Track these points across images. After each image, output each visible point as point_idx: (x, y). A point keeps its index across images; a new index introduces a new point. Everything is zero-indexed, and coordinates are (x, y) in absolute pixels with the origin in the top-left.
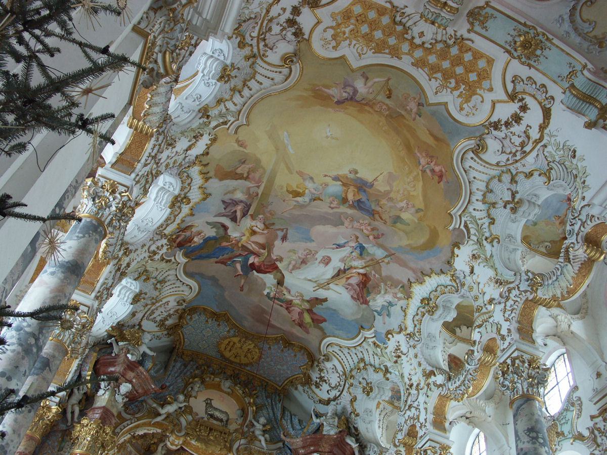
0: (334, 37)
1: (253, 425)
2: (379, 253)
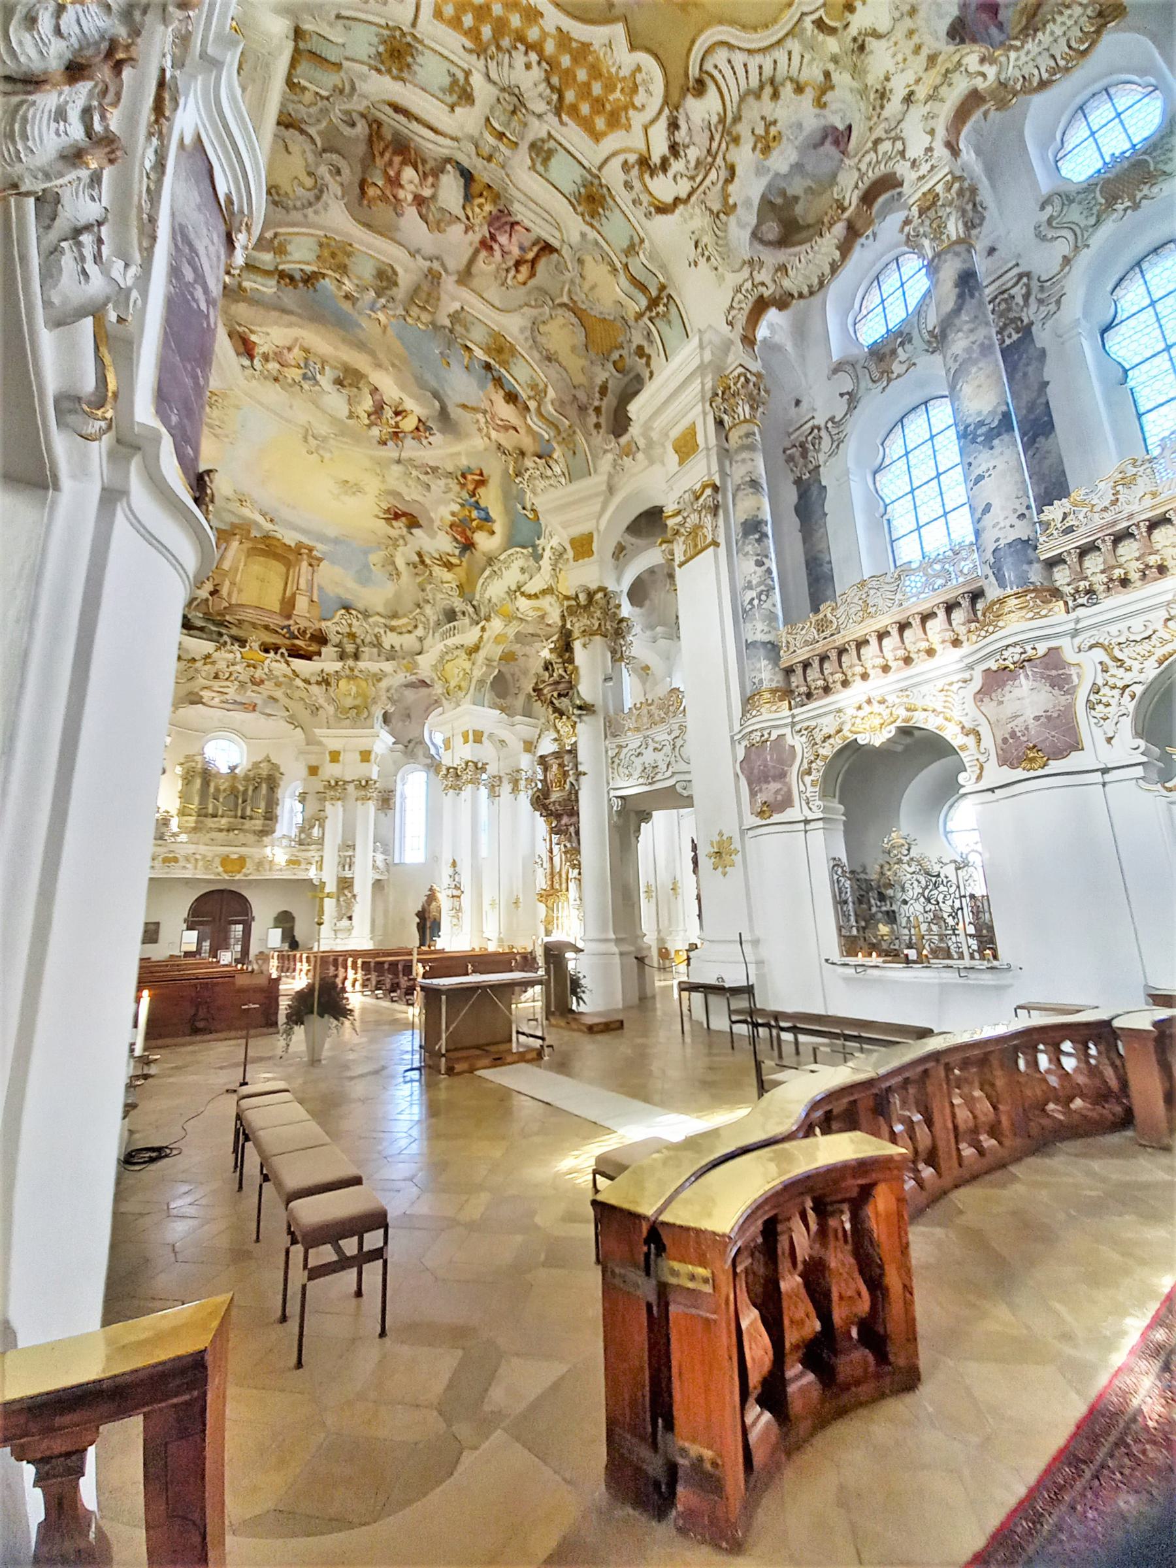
0: (635, 89)
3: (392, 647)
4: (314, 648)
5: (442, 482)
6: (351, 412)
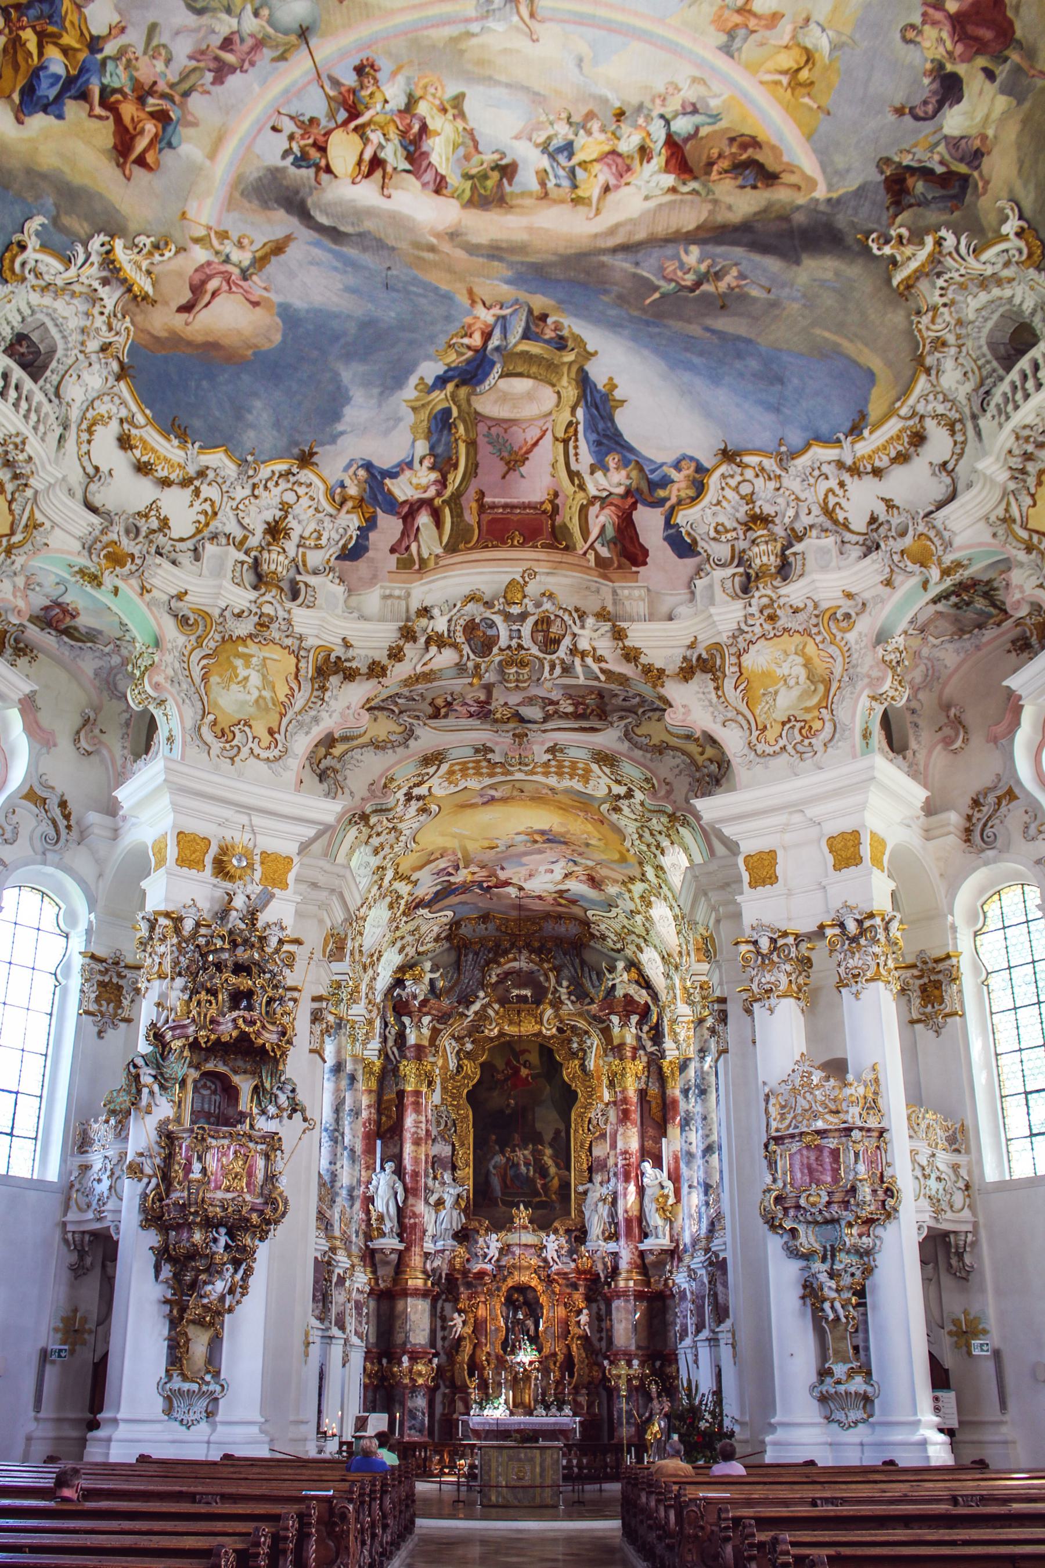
1: (556, 991)
2: (590, 863)
5: (182, 50)
6: (461, 115)
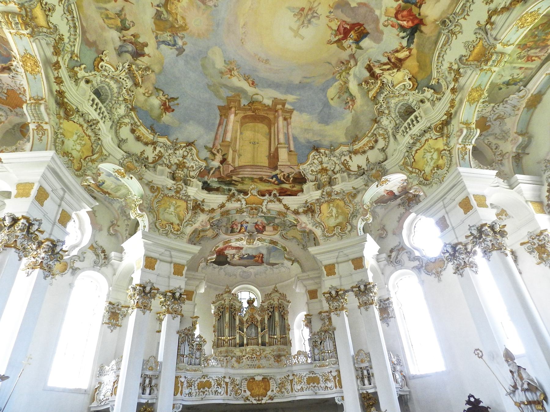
3: (359, 167)
4: (297, 188)
